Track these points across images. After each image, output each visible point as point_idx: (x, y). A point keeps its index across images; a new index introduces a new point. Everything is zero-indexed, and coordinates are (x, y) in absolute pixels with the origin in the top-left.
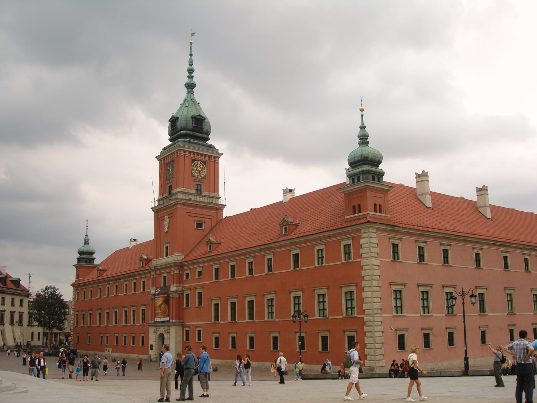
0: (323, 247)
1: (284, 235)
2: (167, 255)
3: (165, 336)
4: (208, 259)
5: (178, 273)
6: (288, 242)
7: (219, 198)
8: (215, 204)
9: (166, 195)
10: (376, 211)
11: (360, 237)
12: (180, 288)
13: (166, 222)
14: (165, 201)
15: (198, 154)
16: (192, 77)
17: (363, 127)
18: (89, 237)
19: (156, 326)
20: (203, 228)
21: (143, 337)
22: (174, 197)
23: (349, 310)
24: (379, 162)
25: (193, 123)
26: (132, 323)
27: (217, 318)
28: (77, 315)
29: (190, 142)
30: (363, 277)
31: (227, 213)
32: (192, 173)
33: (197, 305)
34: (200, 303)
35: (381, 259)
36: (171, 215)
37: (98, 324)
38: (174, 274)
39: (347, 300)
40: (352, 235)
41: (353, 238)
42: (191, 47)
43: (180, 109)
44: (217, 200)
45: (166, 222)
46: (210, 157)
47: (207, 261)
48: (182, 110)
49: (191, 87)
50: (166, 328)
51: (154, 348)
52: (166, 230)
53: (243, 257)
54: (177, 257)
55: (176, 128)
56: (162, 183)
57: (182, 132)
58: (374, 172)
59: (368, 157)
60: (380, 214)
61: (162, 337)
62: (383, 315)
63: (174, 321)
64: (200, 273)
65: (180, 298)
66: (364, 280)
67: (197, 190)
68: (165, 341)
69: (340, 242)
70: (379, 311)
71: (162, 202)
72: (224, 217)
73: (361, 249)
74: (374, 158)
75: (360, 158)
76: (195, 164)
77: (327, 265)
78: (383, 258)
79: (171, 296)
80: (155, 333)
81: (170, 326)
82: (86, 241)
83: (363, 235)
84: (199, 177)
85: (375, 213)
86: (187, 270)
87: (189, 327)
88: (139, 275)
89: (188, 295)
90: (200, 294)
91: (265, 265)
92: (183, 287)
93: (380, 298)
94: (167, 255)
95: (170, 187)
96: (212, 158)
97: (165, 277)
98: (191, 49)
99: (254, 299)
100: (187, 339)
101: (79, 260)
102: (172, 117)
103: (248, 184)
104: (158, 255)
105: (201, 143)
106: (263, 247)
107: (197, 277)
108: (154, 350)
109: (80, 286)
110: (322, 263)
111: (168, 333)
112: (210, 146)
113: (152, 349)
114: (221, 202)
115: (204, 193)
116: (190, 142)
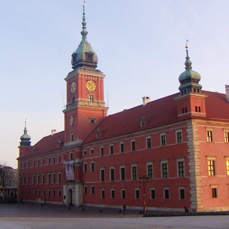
0: (165, 134)
1: (142, 127)
2: (72, 140)
3: (73, 190)
4: (97, 142)
5: (79, 151)
6: (144, 131)
7: (104, 103)
8: (101, 107)
9: (71, 103)
10: (196, 111)
11: (187, 128)
12: (81, 161)
13: (72, 120)
14: (70, 106)
15: (90, 76)
17: (187, 58)
18: (27, 129)
19: (67, 184)
20: (95, 123)
21: (60, 191)
22: (75, 104)
23: (181, 173)
24: (198, 80)
25: (86, 57)
26: (53, 182)
27: (103, 179)
28: (21, 178)
29: (84, 69)
30: (189, 153)
31: (110, 113)
32: (87, 89)
34: (93, 170)
35: (200, 141)
36: (74, 115)
37: (33, 183)
38: (77, 152)
39: (179, 167)
40: (182, 127)
41: (182, 129)
42: (84, 9)
43: (78, 48)
44: (103, 104)
45: (72, 120)
46: (98, 77)
47: (97, 144)
48: (79, 49)
49: (84, 34)
50: (73, 185)
51: (66, 198)
52: (72, 125)
53: (118, 141)
54: (78, 141)
55: (76, 60)
56: (69, 94)
57: (80, 63)
58: (196, 86)
59: (191, 77)
60: (199, 113)
61: (71, 191)
62: (202, 176)
63: (78, 181)
64: (92, 151)
65: (81, 168)
66: (189, 155)
67: (91, 99)
68: (73, 193)
69: (175, 131)
70: (199, 174)
71: (68, 107)
72: (108, 115)
73: (187, 136)
74: (195, 78)
75: (185, 78)
76: (88, 83)
77: (167, 145)
78: (201, 140)
79: (75, 166)
80: (67, 188)
81: (75, 184)
82: (25, 131)
83: (189, 127)
84: (91, 91)
85: (196, 113)
88: (57, 152)
89: (86, 165)
90: (93, 164)
91: (130, 145)
93: (200, 166)
94: (72, 140)
95: (74, 97)
96: (99, 79)
97: (72, 154)
99: (114, 168)
100: (86, 192)
101: (21, 143)
102: (73, 54)
103: (121, 96)
104: (68, 140)
105: (92, 69)
106: (129, 135)
107: (91, 153)
108: (66, 199)
109: (22, 160)
110: (165, 145)
111: (74, 188)
112: (98, 71)
113: (65, 198)
114: (106, 106)
115: (95, 101)
116: (84, 69)
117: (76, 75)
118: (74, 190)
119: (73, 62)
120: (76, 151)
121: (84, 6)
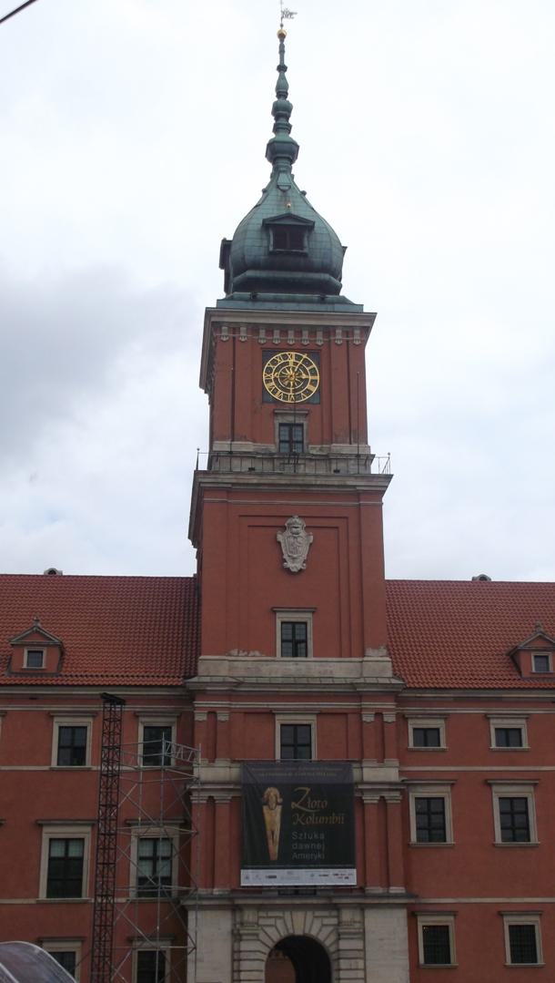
16: (288, 128)
19: (260, 908)
33: (498, 840)
49: (282, 153)
50: (347, 915)
63: (394, 890)
64: (509, 736)
79: (371, 799)
81: (362, 908)
86: (431, 716)
87: (454, 914)
88: (33, 698)
92: (401, 773)
98: (282, 51)
102: (290, 216)
107: (494, 746)
111: (362, 935)
117: (348, 332)
118: (359, 945)
119: (271, 254)
120: (368, 718)
121: (282, 36)
